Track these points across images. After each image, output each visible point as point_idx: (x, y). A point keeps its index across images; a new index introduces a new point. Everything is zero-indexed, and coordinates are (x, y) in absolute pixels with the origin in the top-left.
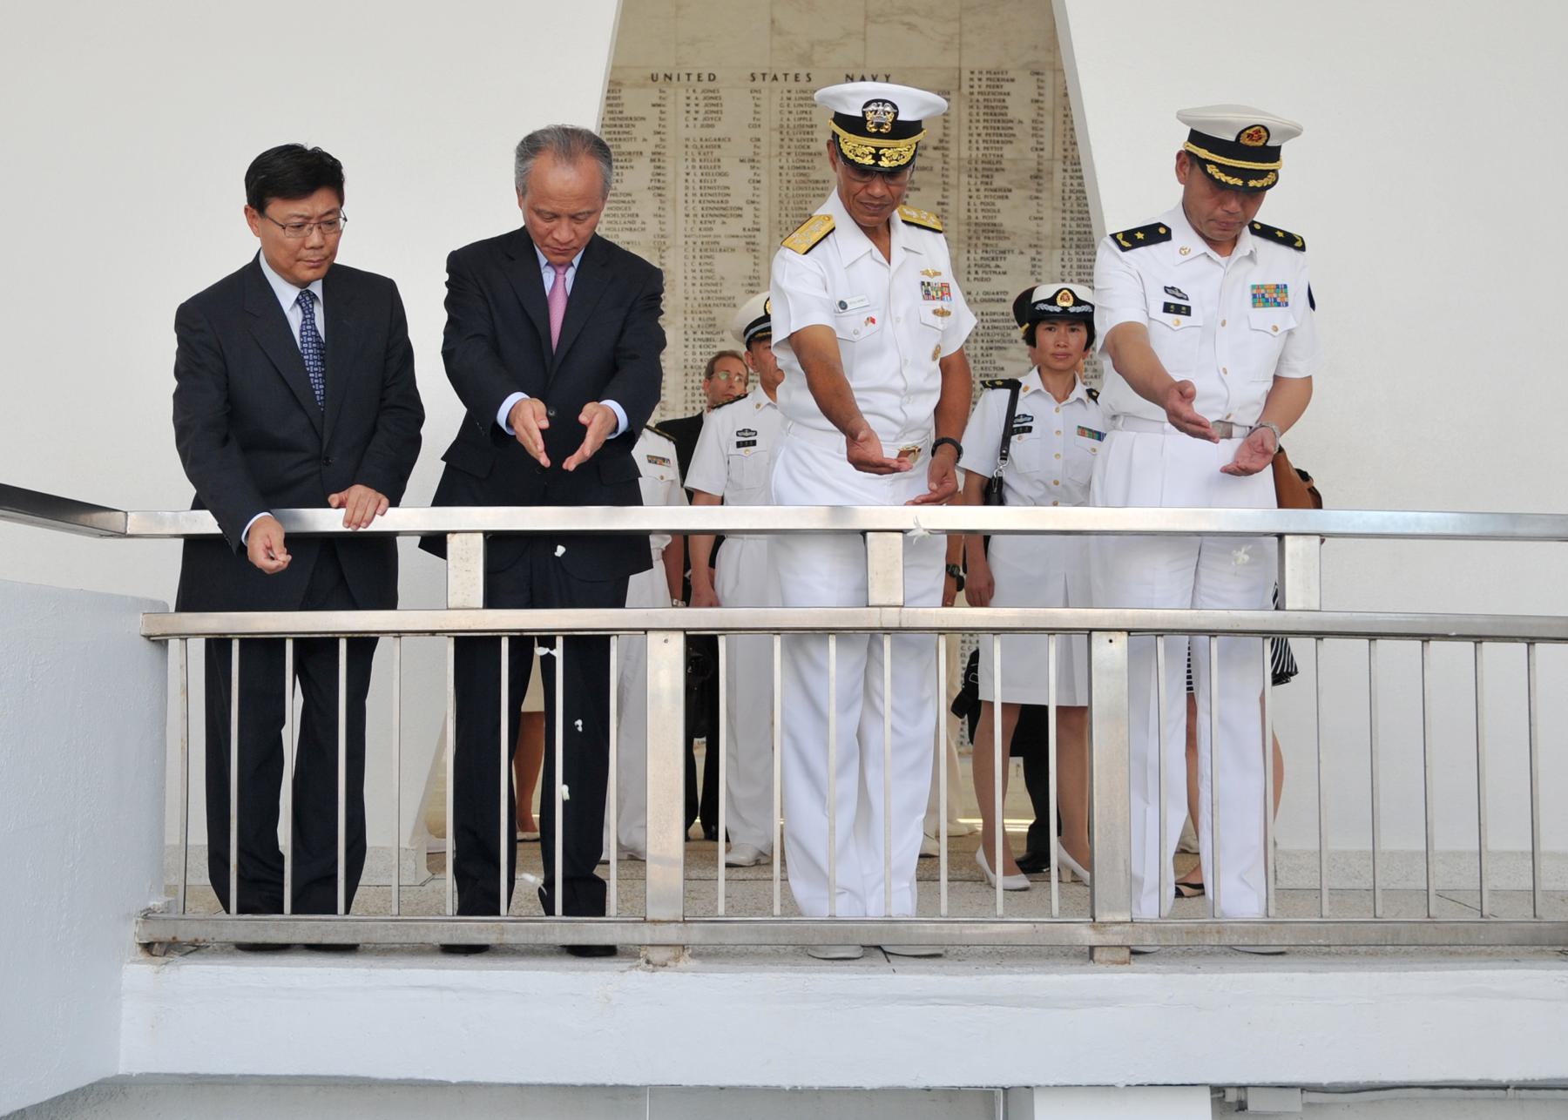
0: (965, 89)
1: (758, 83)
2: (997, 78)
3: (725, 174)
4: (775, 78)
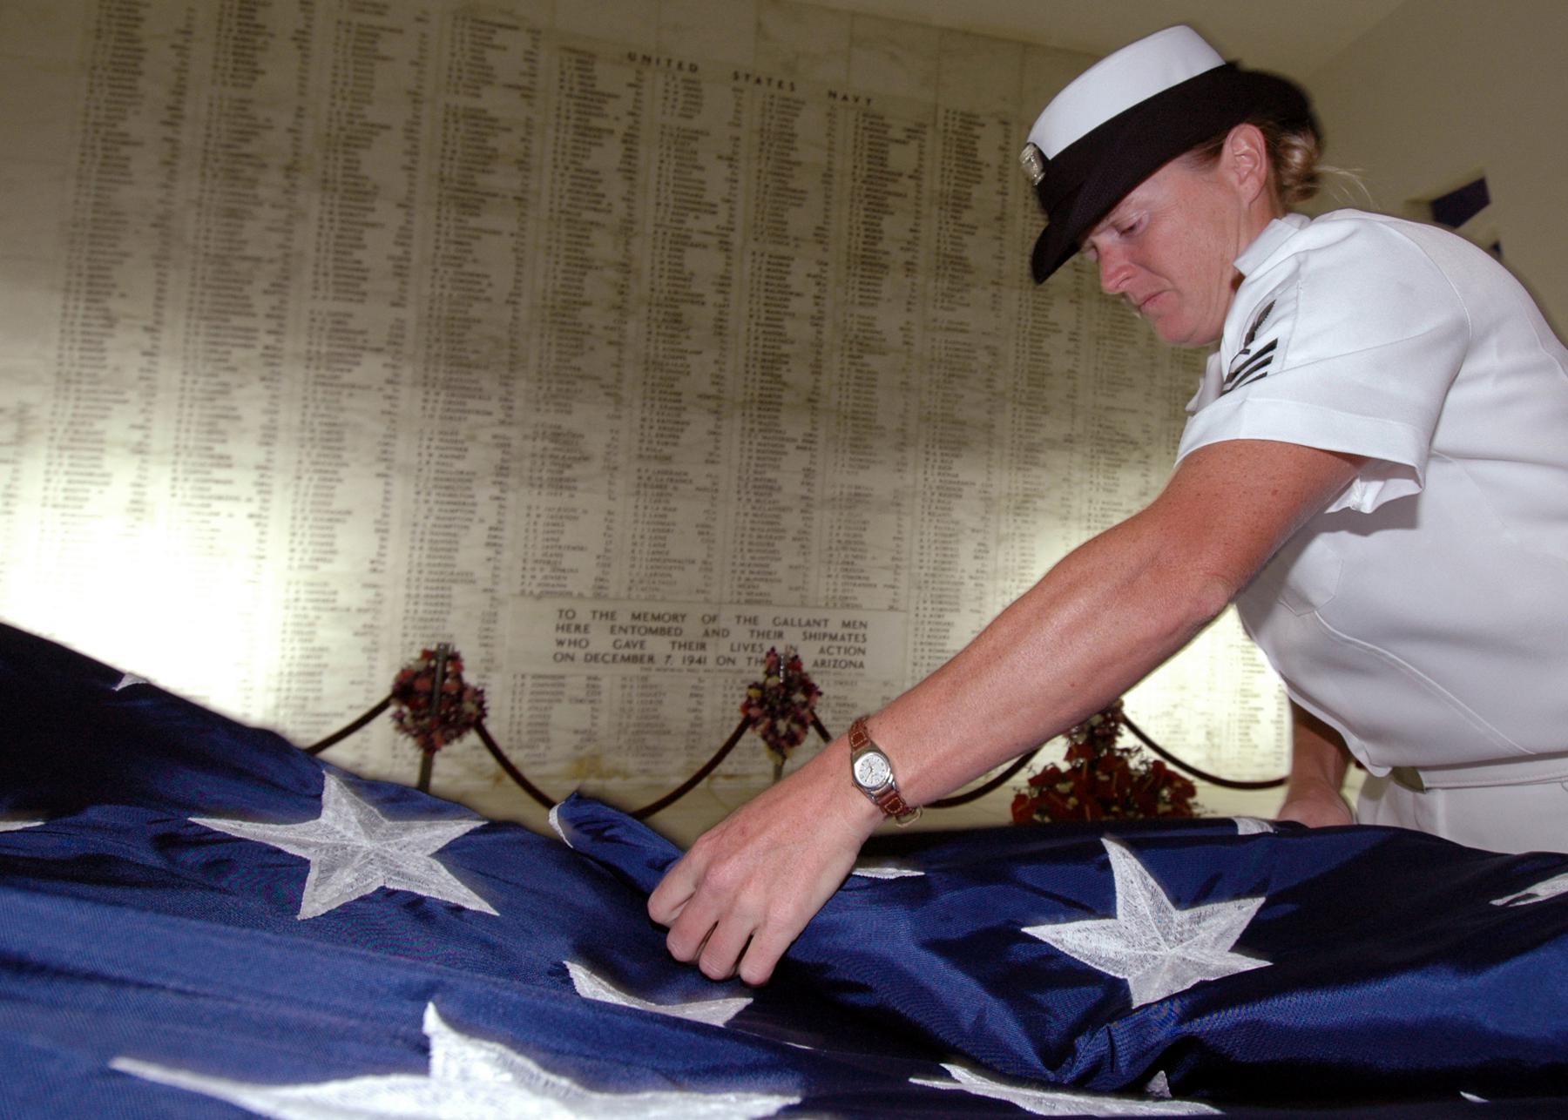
0: (941, 126)
1: (741, 83)
2: (970, 121)
3: (701, 168)
4: (758, 81)
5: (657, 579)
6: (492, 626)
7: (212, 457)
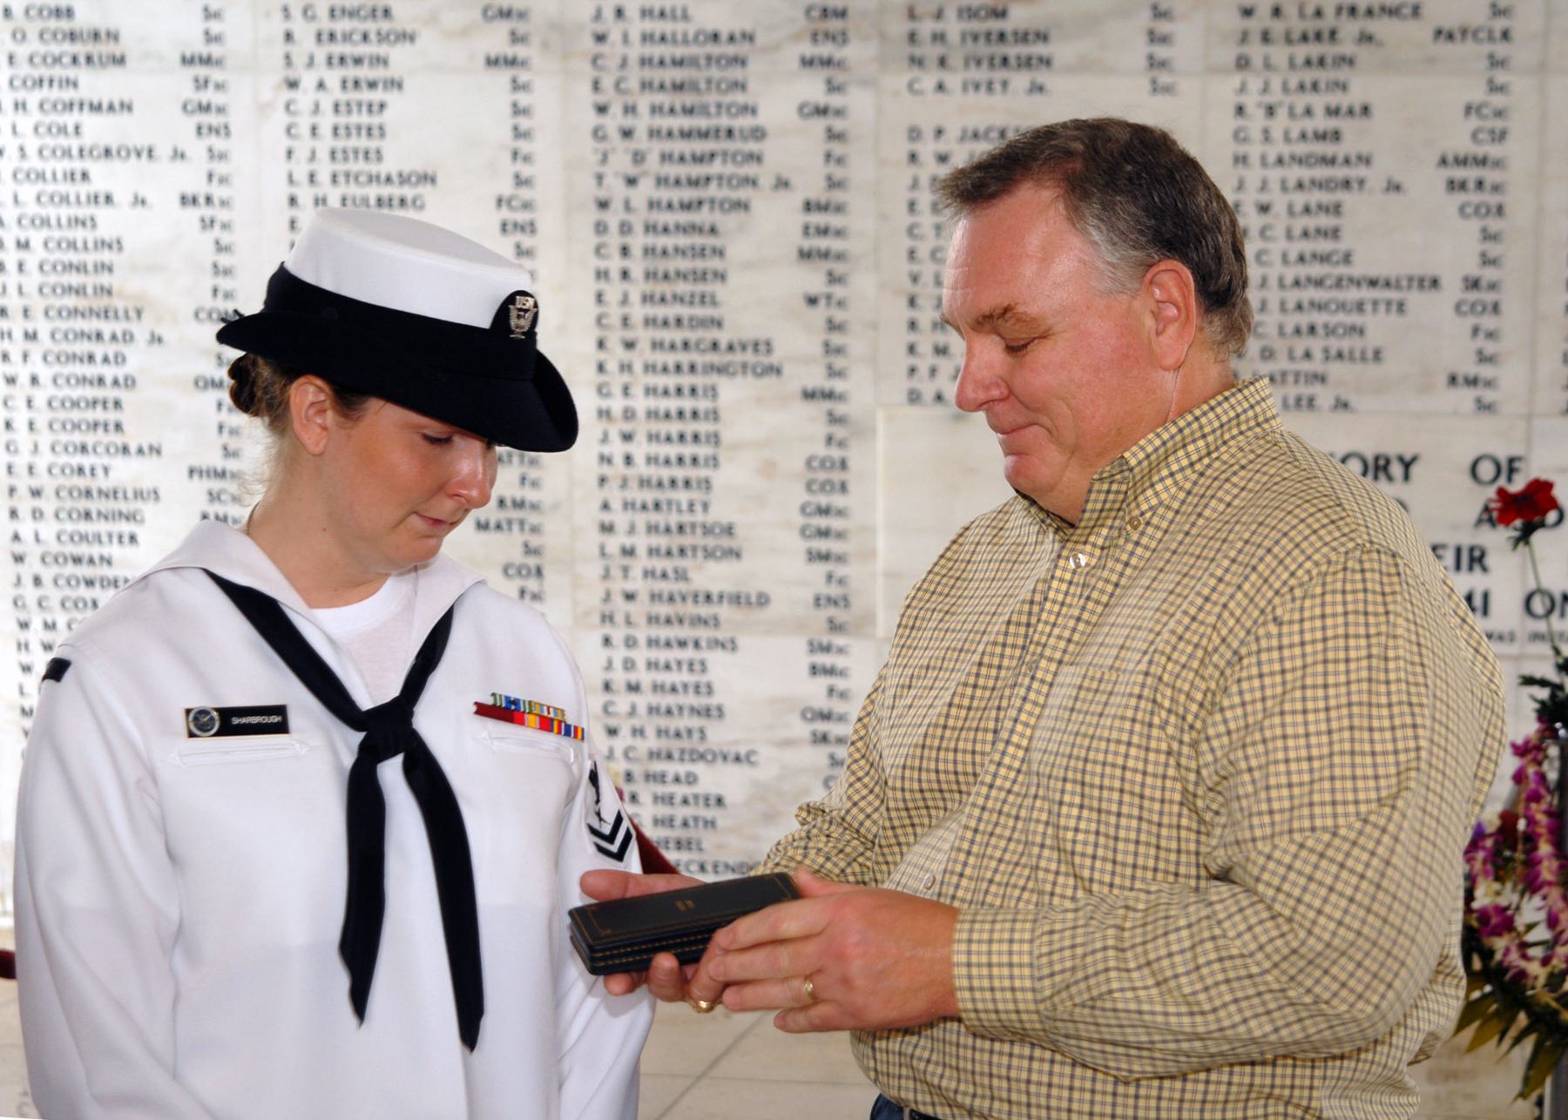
5: (1316, 345)
6: (838, 501)
7: (73, 36)
